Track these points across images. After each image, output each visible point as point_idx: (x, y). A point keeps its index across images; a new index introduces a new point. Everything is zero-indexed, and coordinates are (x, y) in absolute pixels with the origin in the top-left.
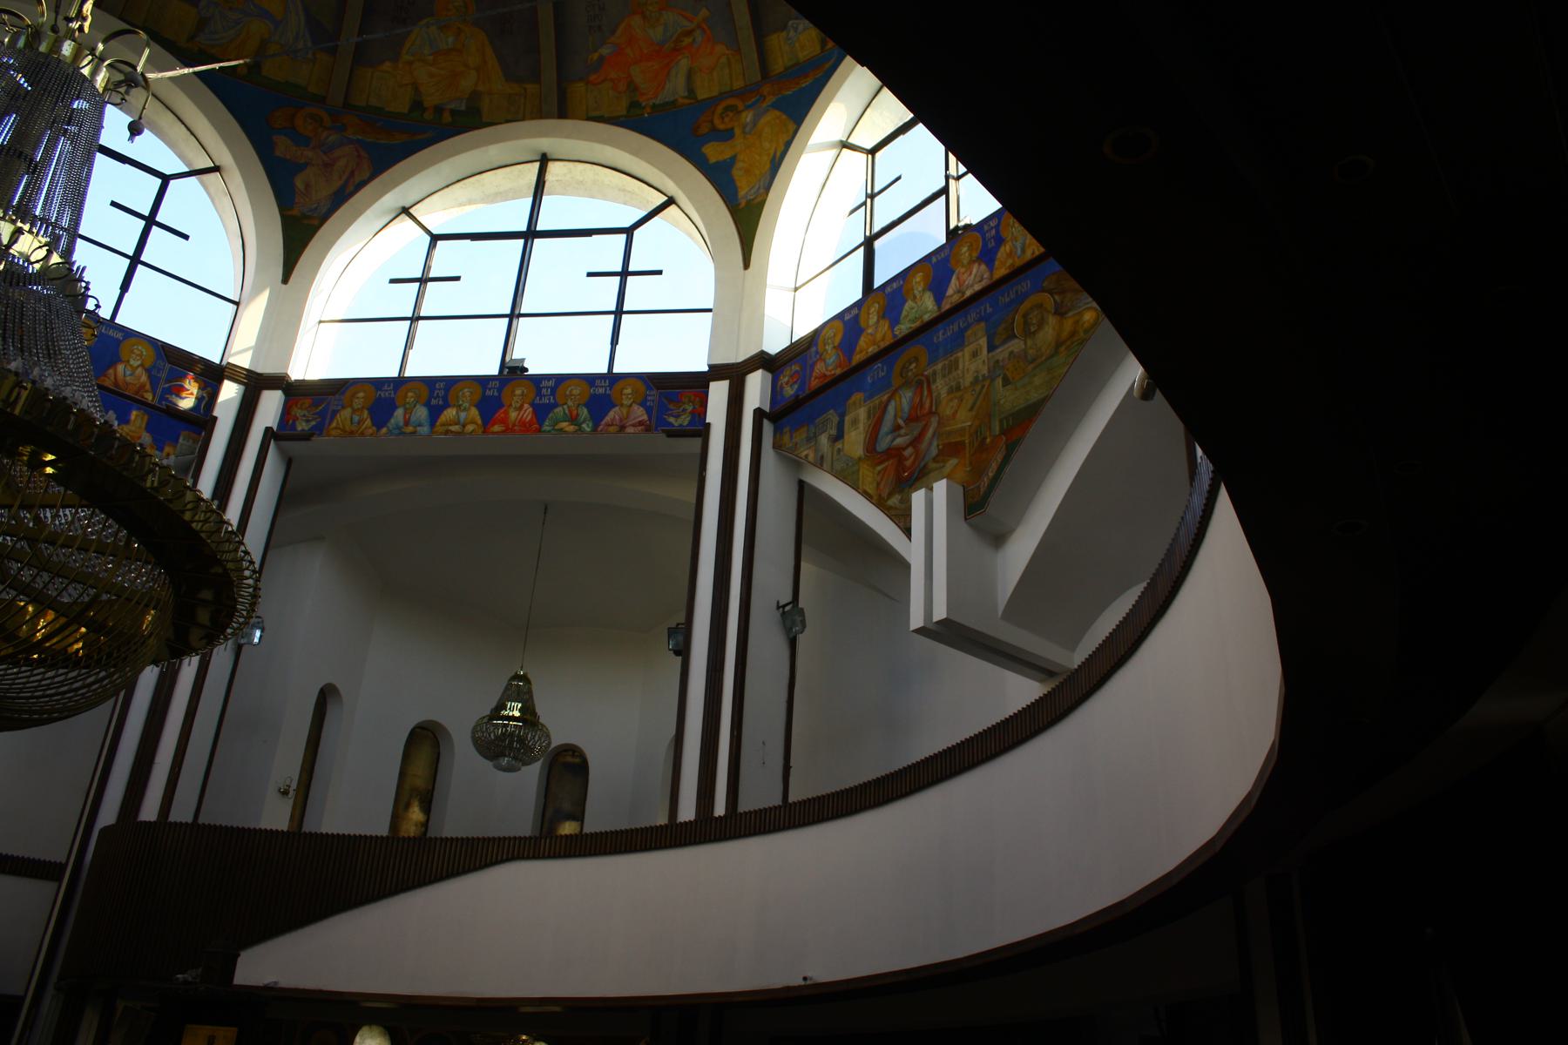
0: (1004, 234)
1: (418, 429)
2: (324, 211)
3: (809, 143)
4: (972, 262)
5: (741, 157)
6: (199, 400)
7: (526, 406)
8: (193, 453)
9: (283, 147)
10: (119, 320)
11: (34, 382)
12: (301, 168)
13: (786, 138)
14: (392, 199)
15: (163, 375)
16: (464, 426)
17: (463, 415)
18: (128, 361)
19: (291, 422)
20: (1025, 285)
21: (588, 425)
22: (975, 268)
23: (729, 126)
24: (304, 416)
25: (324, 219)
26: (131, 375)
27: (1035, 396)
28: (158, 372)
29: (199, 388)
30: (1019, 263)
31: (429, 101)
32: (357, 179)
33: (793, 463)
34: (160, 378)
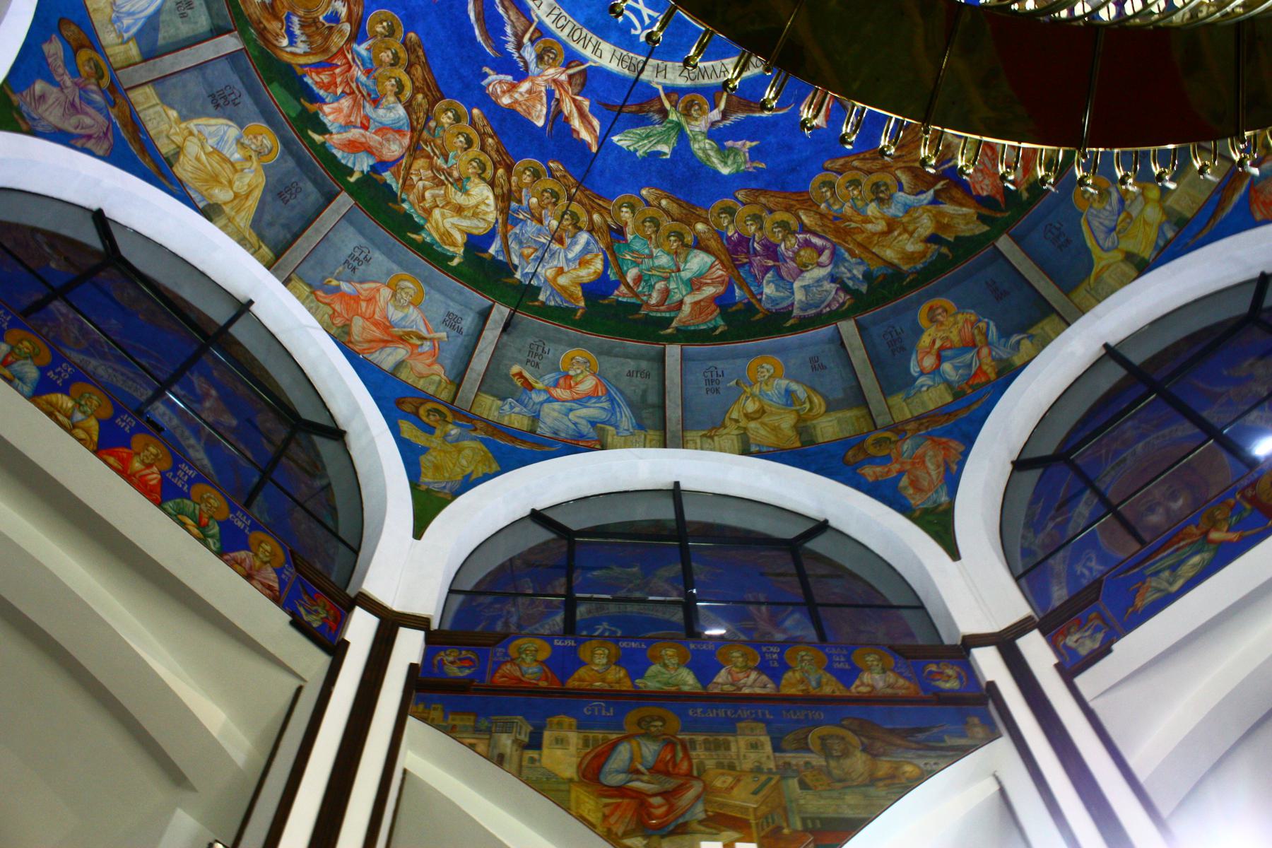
7: (155, 469)
16: (74, 427)
17: (78, 416)
22: (753, 675)
23: (432, 424)
27: (849, 813)
30: (813, 692)
32: (89, 145)
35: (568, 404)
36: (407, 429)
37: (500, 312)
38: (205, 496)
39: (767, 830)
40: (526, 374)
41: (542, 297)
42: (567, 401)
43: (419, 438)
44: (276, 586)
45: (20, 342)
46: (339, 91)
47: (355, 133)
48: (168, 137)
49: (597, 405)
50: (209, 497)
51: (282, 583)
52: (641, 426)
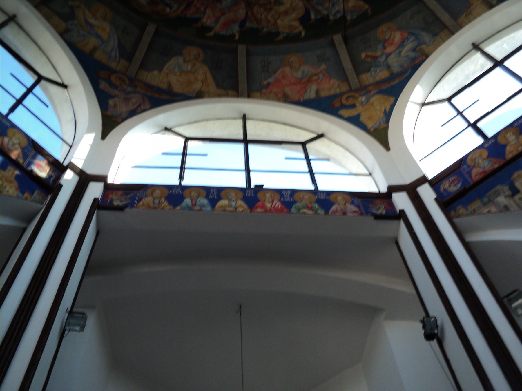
7: (275, 202)
8: (42, 203)
12: (112, 97)
19: (109, 201)
25: (124, 120)
29: (50, 170)
32: (143, 107)
35: (397, 52)
36: (345, 113)
37: (338, 38)
40: (370, 53)
41: (349, 18)
42: (395, 51)
43: (352, 113)
44: (356, 209)
45: (190, 193)
46: (202, 9)
47: (222, 20)
49: (410, 41)
51: (358, 206)
52: (435, 35)
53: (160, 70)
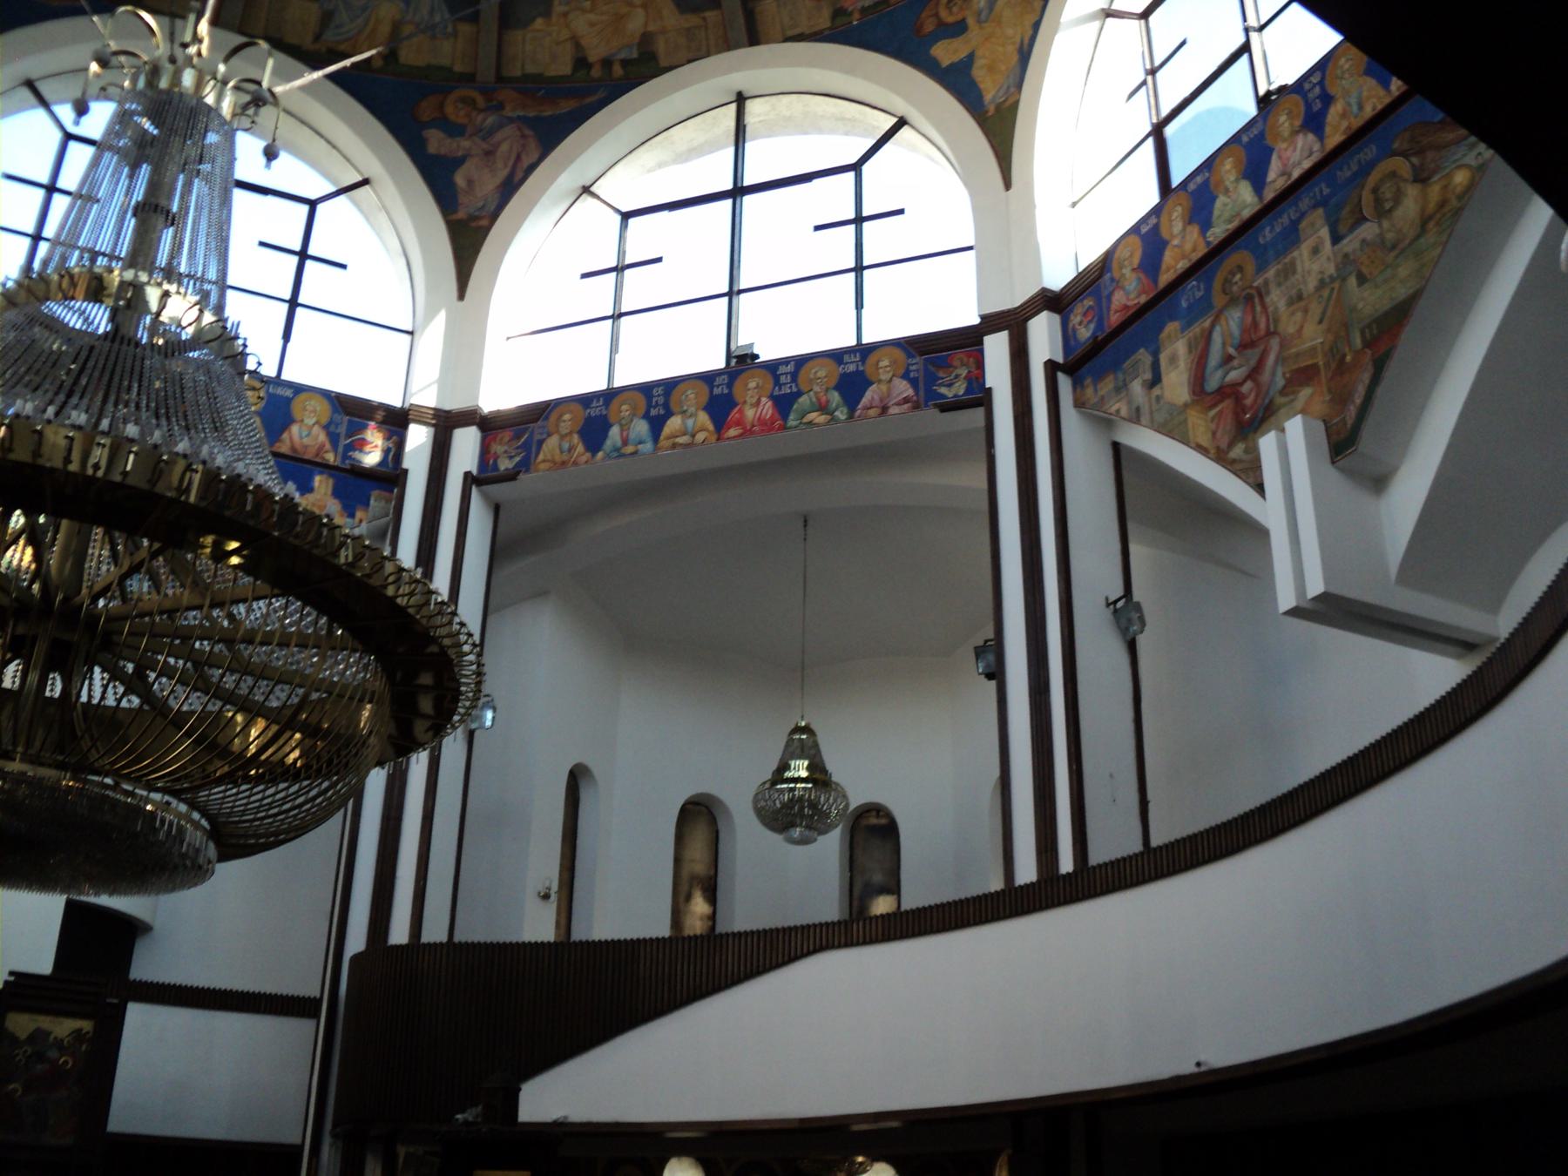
0: (1332, 91)
1: (640, 447)
2: (493, 208)
3: (1062, 20)
4: (1295, 133)
5: (979, 53)
6: (386, 452)
7: (764, 400)
9: (436, 141)
10: (284, 376)
11: (204, 463)
13: (1033, 18)
14: (569, 179)
15: (342, 430)
16: (693, 436)
17: (690, 422)
18: (302, 421)
19: (491, 462)
20: (1370, 152)
21: (842, 412)
23: (959, 17)
24: (506, 452)
25: (494, 217)
26: (308, 435)
27: (1402, 292)
28: (337, 428)
30: (1357, 123)
31: (593, 57)
32: (526, 162)
33: (1105, 423)
34: (338, 435)
38: (812, 376)
39: (1333, 366)
48: (558, 43)
50: (816, 373)
53: (547, 14)
